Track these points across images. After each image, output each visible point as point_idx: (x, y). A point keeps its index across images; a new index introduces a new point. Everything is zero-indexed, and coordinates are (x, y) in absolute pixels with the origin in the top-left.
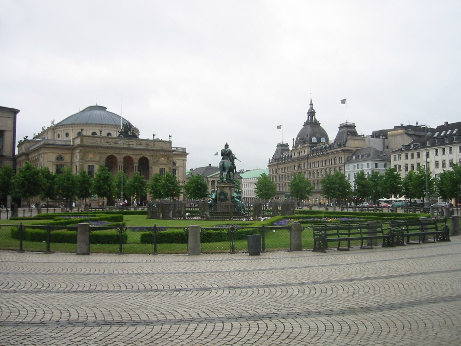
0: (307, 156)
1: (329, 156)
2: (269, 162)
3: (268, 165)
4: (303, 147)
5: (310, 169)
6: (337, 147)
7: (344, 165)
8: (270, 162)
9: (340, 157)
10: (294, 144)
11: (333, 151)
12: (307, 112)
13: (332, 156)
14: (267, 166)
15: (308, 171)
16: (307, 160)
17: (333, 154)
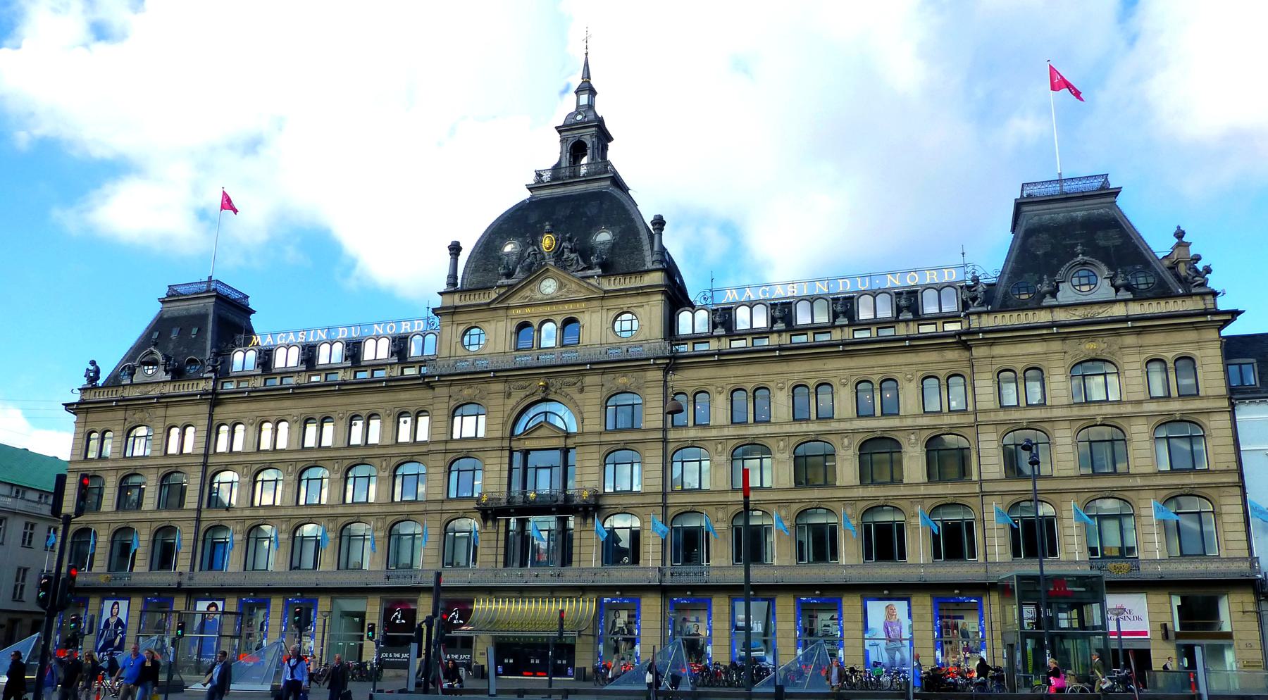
0: (661, 347)
1: (998, 350)
2: (83, 382)
3: (76, 398)
4: (605, 296)
5: (693, 433)
6: (1110, 293)
7: (1233, 406)
8: (100, 382)
9: (1169, 356)
10: (453, 276)
11: (1061, 316)
12: (561, 123)
13: (1037, 347)
14: (68, 406)
15: (665, 441)
16: (658, 375)
17: (1065, 337)
